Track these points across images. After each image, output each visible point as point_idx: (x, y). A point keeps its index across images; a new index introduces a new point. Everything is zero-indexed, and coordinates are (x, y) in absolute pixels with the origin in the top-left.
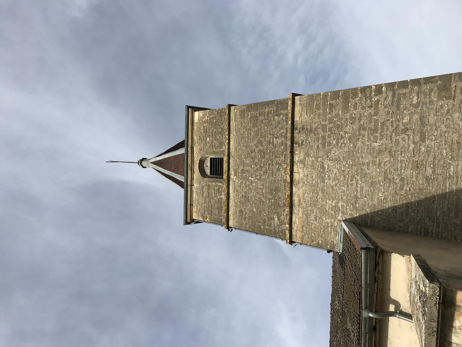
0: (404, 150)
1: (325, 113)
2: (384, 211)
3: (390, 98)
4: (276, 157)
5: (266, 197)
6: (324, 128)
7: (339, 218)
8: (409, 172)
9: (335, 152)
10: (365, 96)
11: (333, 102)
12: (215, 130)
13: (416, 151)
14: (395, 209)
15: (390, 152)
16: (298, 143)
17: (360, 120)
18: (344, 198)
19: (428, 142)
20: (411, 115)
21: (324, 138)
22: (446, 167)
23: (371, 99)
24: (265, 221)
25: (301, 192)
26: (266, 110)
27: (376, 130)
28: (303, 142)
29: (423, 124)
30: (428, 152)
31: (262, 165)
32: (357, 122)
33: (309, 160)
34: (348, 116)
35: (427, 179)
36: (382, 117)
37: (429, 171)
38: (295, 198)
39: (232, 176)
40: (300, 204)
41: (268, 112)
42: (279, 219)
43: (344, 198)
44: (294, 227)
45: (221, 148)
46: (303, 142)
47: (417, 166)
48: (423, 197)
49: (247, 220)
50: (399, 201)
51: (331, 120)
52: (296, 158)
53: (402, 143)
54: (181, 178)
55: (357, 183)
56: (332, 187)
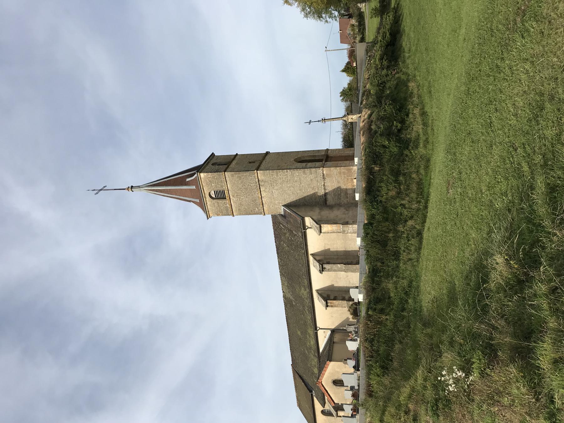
0: (297, 186)
1: (270, 176)
2: (294, 201)
3: (290, 173)
4: (253, 190)
5: (251, 203)
6: (271, 181)
7: (281, 205)
8: (298, 192)
9: (276, 188)
10: (283, 172)
11: (273, 174)
12: (216, 181)
13: (300, 186)
14: (296, 200)
15: (293, 187)
16: (261, 185)
17: (282, 179)
18: (281, 200)
19: (302, 184)
20: (297, 178)
21: (271, 183)
22: (307, 190)
23: (285, 173)
24: (252, 211)
25: (265, 199)
26: (245, 174)
27: (288, 182)
28: (263, 185)
29: (300, 180)
30: (303, 186)
31: (247, 193)
32: (282, 179)
33: (267, 190)
34: (278, 177)
35: (303, 193)
36: (289, 178)
37: (304, 191)
38: (264, 202)
39: (231, 197)
40: (266, 203)
41: (246, 175)
42: (258, 209)
43: (281, 200)
44: (265, 210)
45: (222, 188)
46: (263, 185)
47: (300, 190)
48: (303, 197)
49: (243, 212)
50: (297, 198)
51: (273, 179)
52: (262, 190)
53: (296, 185)
54: (198, 201)
55: (284, 195)
56: (277, 197)
